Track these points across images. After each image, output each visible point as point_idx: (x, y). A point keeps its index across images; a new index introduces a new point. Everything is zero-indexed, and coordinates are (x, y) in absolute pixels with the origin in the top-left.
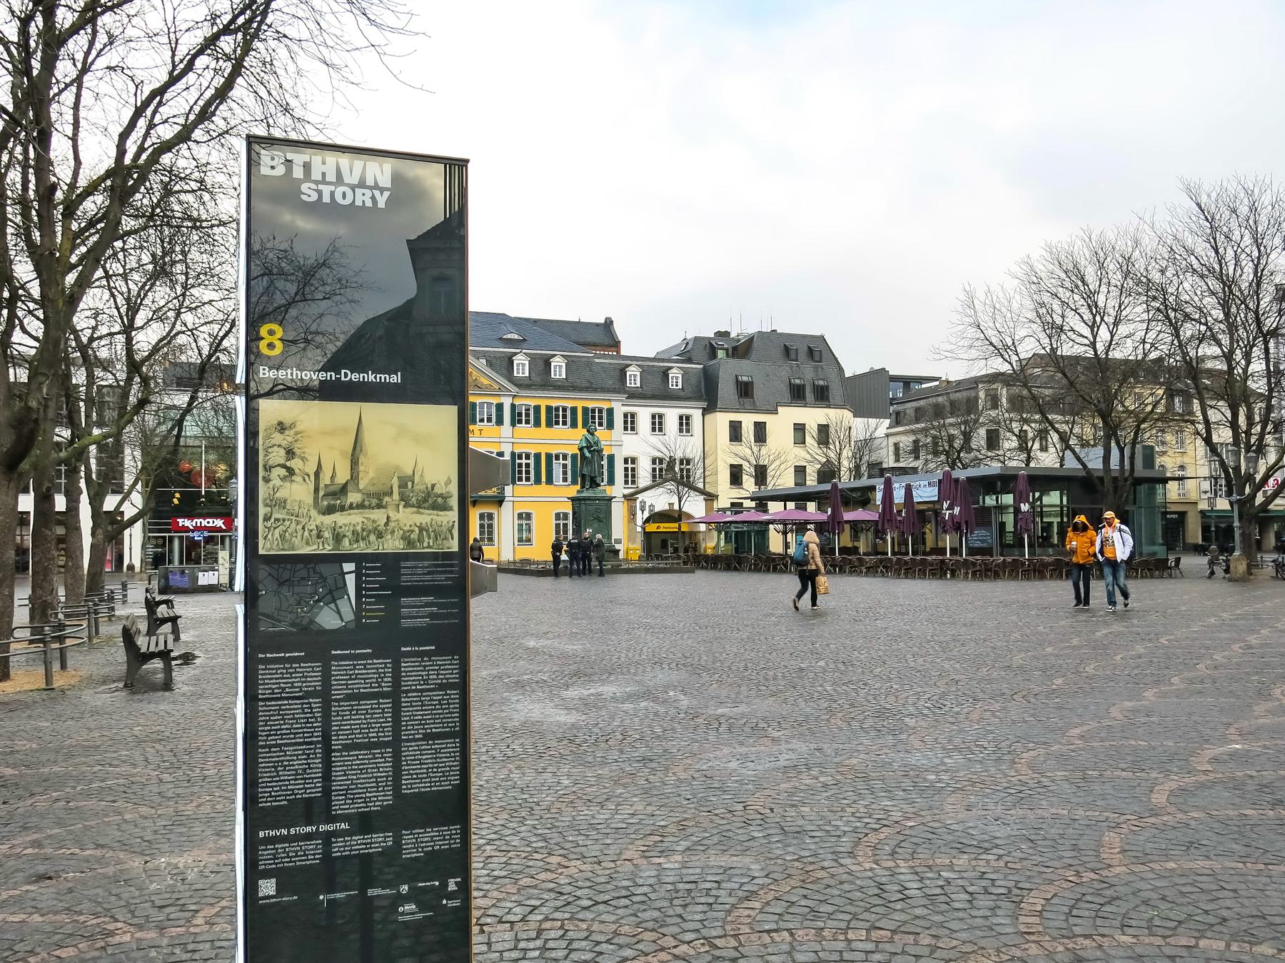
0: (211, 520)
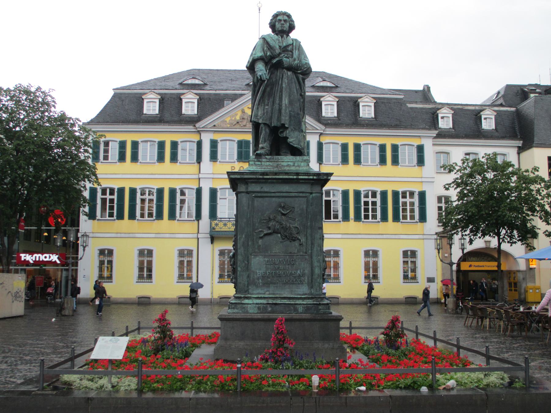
0: (47, 255)
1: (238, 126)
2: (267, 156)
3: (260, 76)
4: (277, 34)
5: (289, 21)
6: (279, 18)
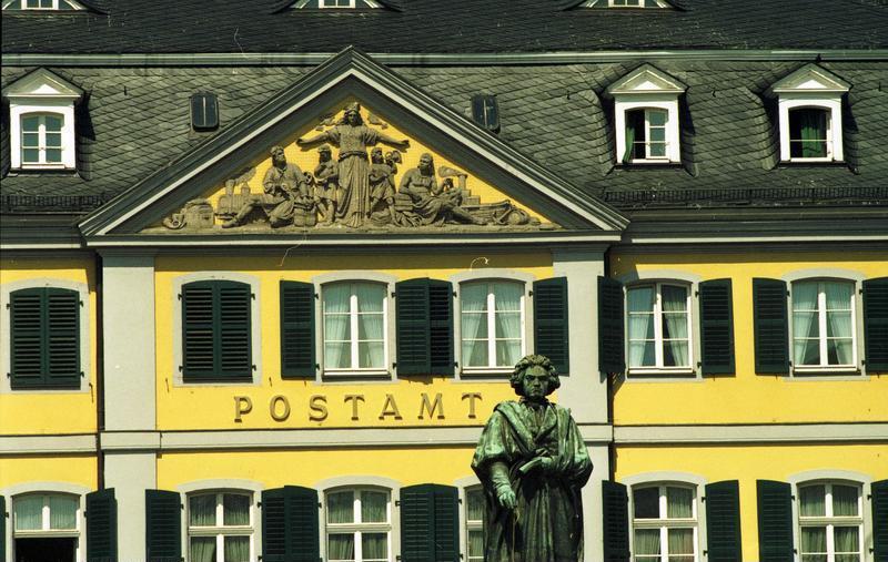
1: (258, 227)
6: (529, 372)
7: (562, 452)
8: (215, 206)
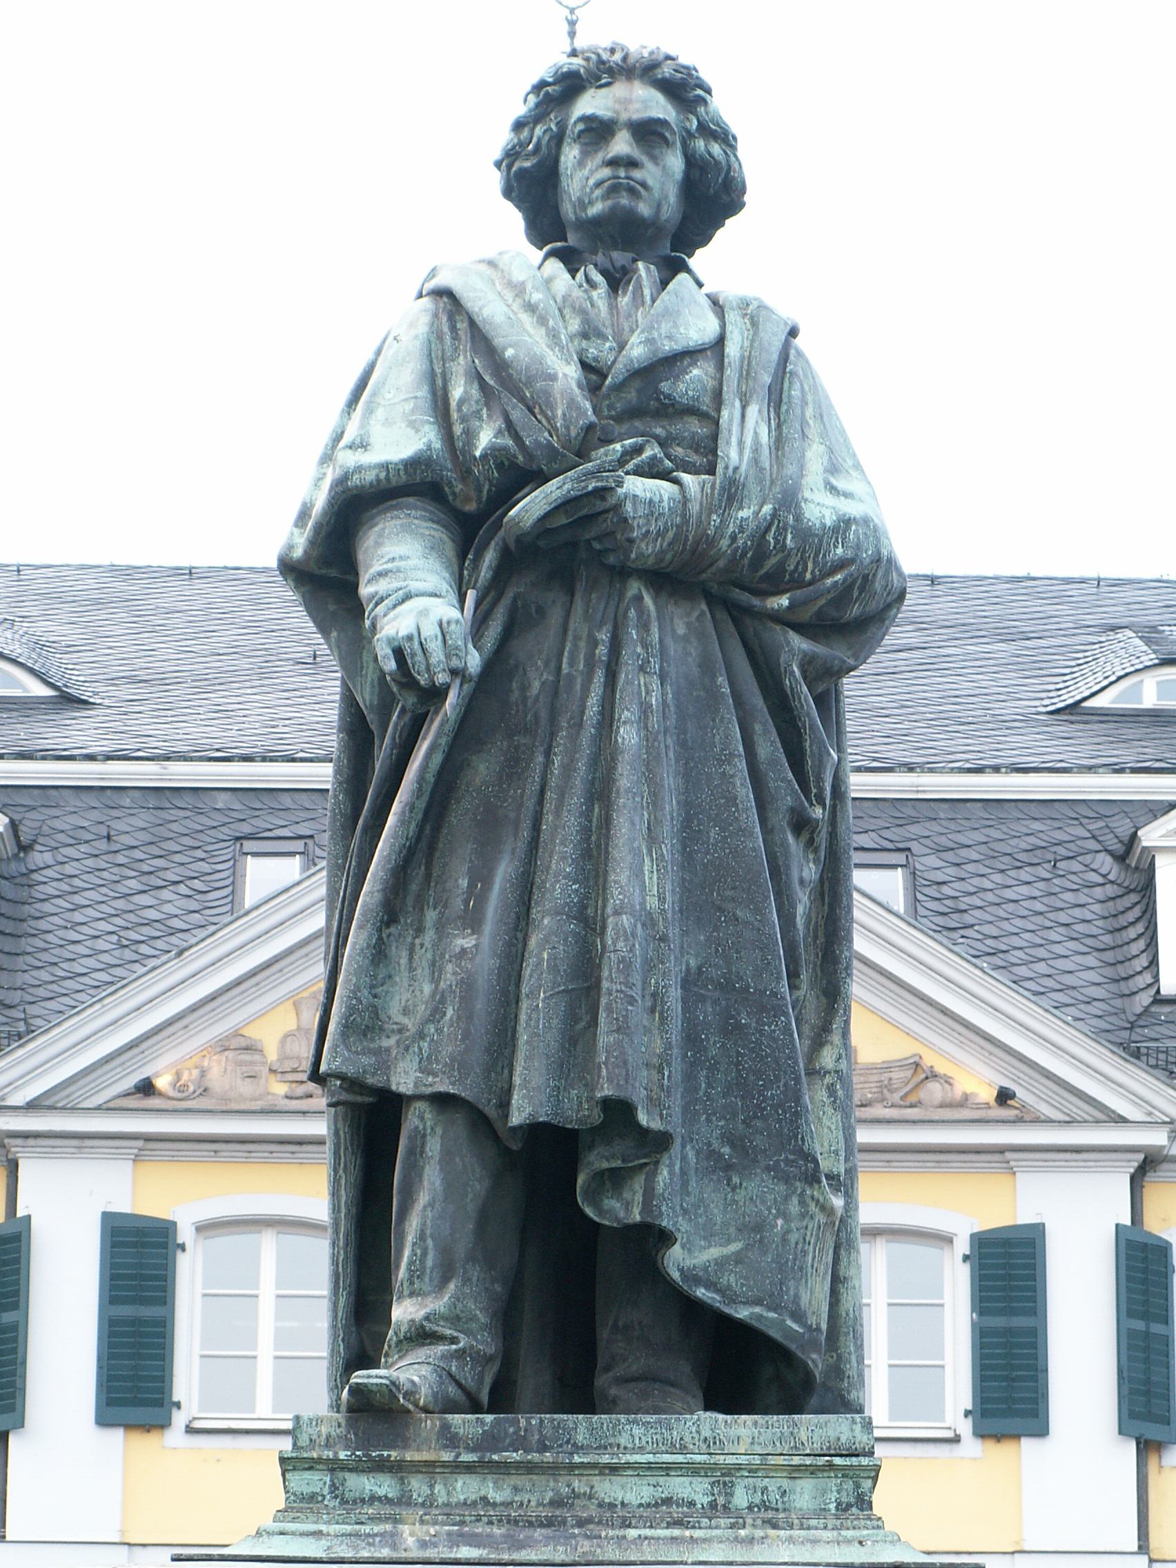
2: (456, 1419)
3: (399, 653)
4: (571, 260)
5: (688, 136)
6: (590, 104)
7: (732, 454)
8: (272, 1055)
